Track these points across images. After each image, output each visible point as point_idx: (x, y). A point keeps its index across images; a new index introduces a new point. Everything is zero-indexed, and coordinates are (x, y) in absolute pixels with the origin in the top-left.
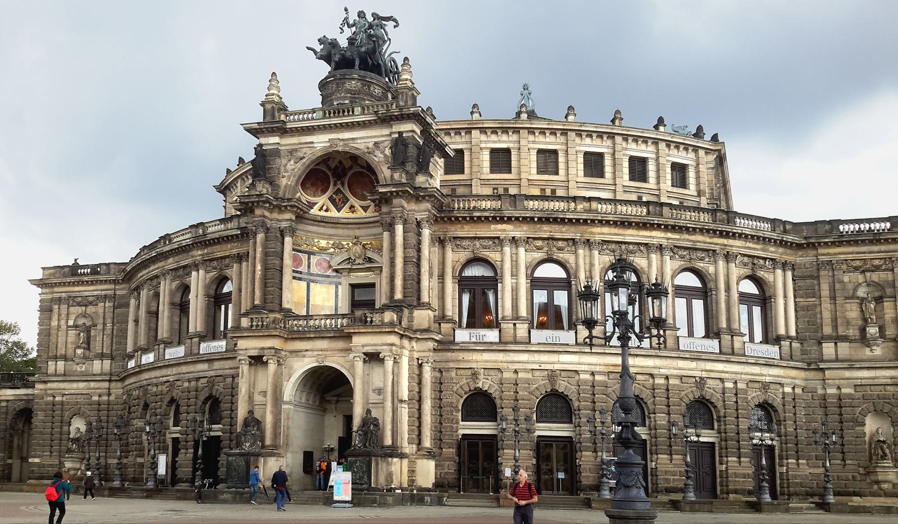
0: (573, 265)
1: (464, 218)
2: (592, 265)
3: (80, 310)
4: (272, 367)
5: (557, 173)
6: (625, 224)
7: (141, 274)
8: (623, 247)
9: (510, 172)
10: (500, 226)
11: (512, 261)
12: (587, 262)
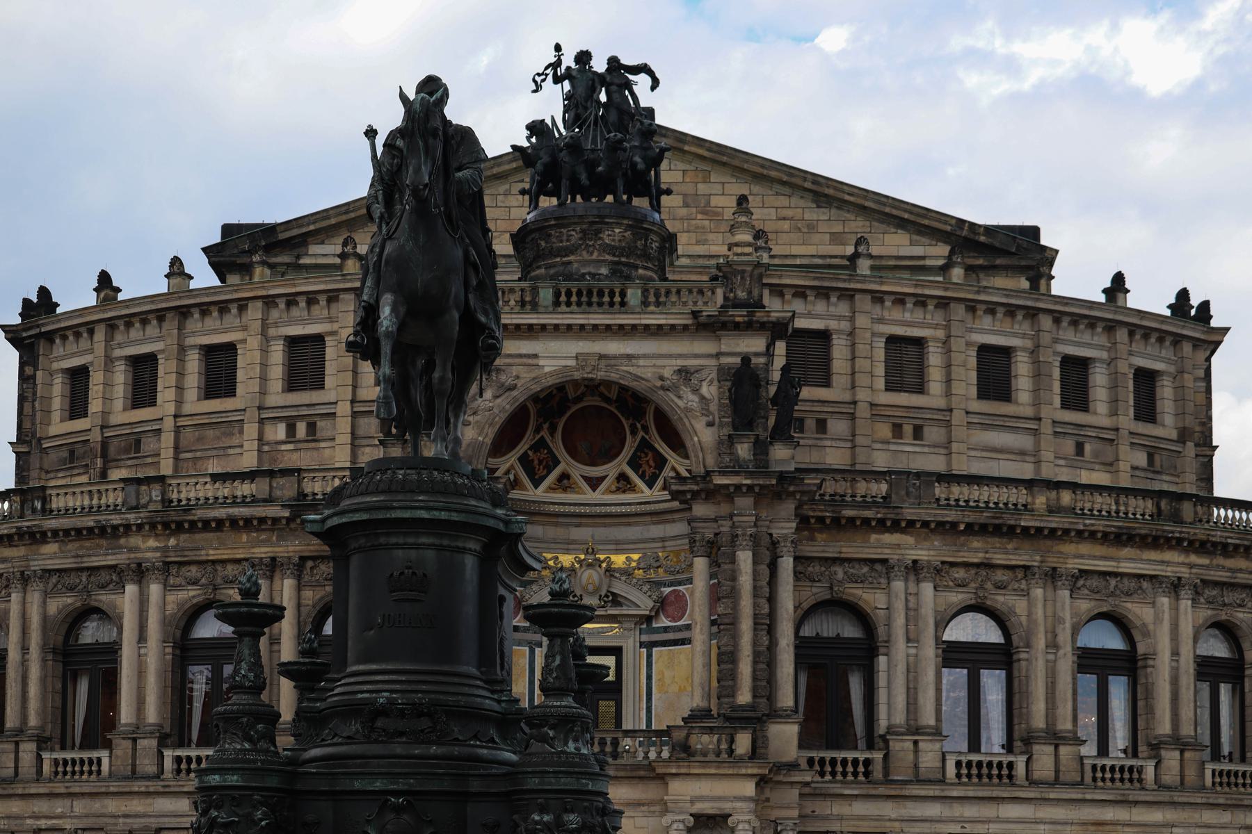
0: (1024, 619)
1: (821, 520)
5: (920, 389)
6: (1120, 539)
8: (1113, 582)
9: (827, 383)
10: (888, 538)
11: (907, 609)
12: (1049, 613)
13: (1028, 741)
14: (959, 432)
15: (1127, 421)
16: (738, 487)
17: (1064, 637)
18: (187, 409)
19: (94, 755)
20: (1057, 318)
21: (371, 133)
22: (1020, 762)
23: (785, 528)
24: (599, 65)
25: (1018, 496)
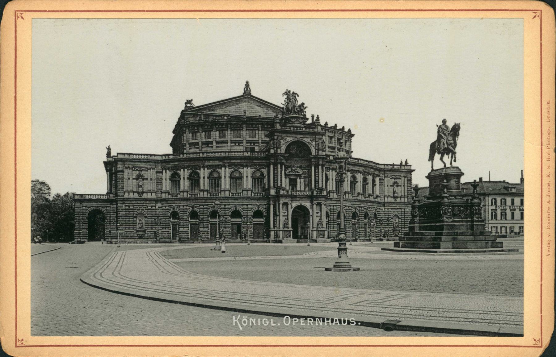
3: (138, 172)
4: (290, 206)
13: (345, 193)
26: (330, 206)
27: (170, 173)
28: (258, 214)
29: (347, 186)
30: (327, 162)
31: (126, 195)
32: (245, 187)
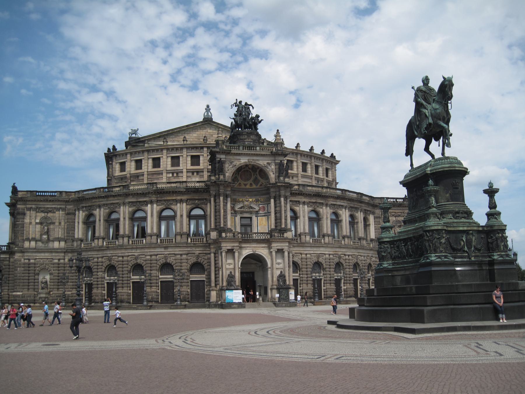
2: (327, 213)
3: (43, 215)
4: (236, 254)
7: (97, 200)
10: (300, 197)
13: (324, 236)
14: (300, 178)
15: (325, 177)
16: (282, 186)
17: (329, 216)
18: (149, 170)
19: (142, 239)
20: (315, 157)
21: (413, 88)
22: (323, 240)
23: (288, 194)
24: (243, 104)
25: (320, 189)
26: (301, 254)
27: (84, 214)
28: (197, 267)
29: (327, 226)
30: (293, 194)
31: (27, 244)
32: (178, 231)
